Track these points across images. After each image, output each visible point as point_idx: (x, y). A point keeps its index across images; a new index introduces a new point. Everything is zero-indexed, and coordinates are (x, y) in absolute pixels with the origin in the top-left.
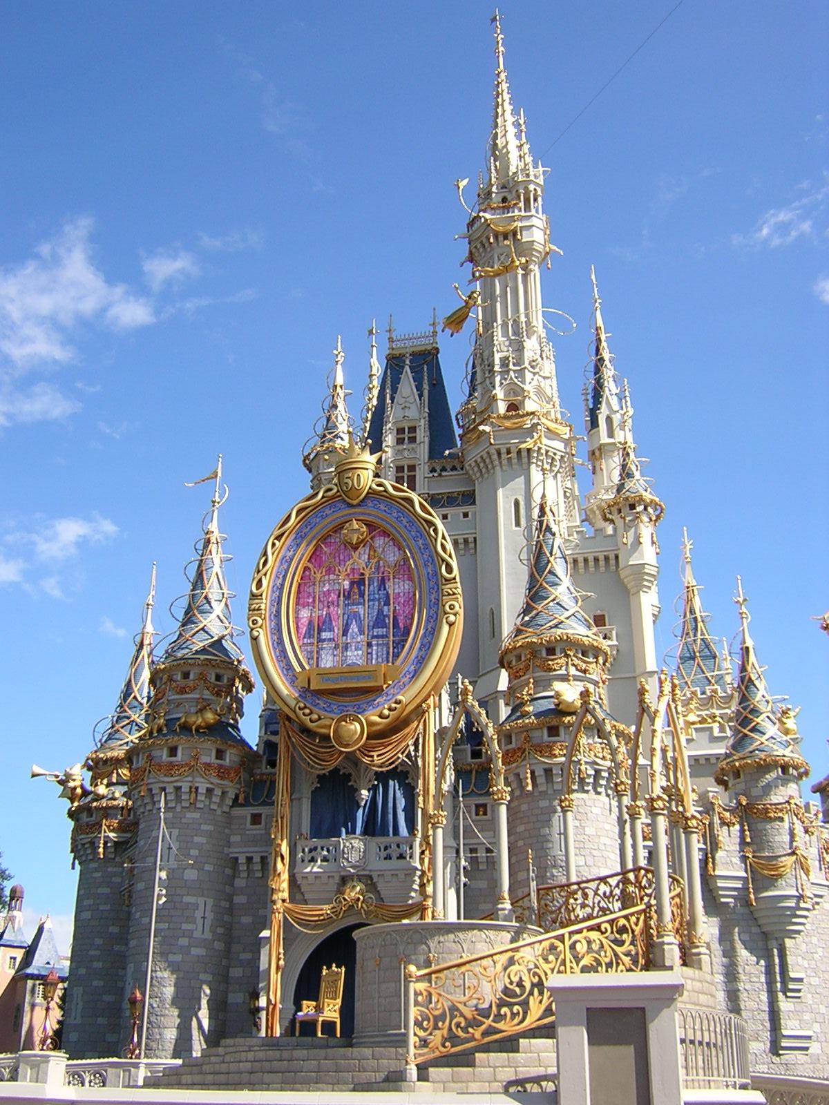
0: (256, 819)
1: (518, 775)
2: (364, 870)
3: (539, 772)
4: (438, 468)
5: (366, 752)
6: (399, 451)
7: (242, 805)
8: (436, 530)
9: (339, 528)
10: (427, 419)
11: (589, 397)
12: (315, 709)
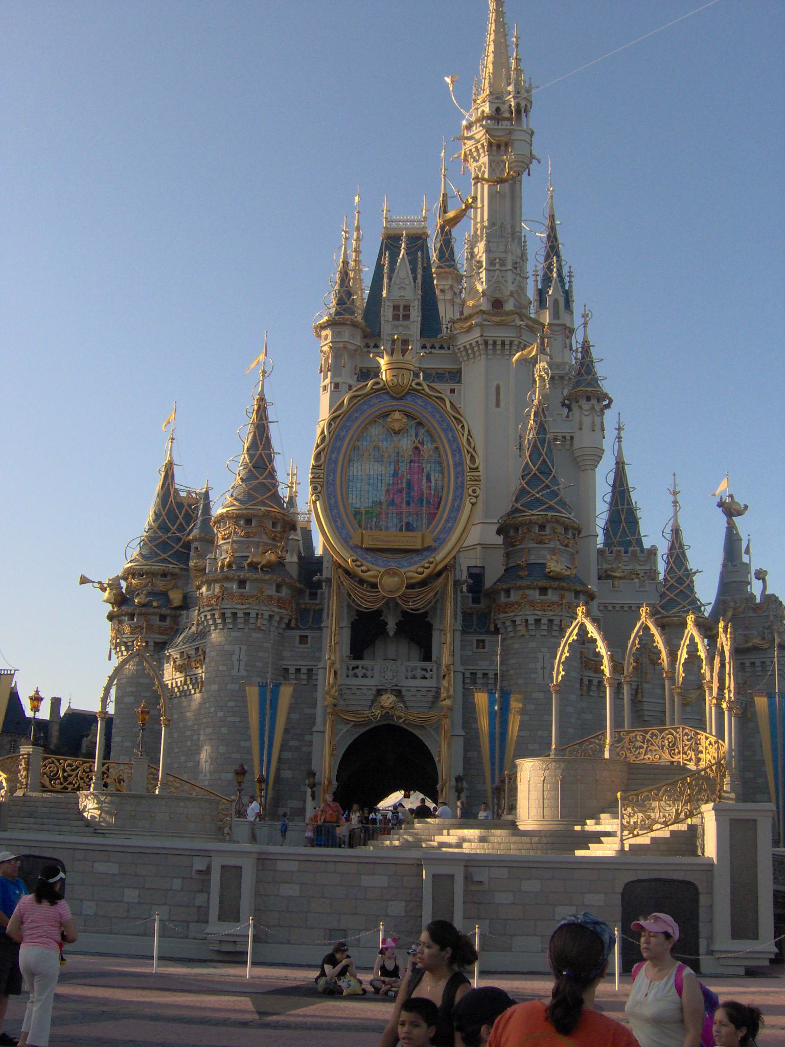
0: (303, 639)
2: (396, 686)
4: (428, 346)
5: (404, 598)
6: (395, 326)
7: (292, 629)
9: (386, 415)
10: (420, 300)
11: (539, 278)
12: (365, 563)
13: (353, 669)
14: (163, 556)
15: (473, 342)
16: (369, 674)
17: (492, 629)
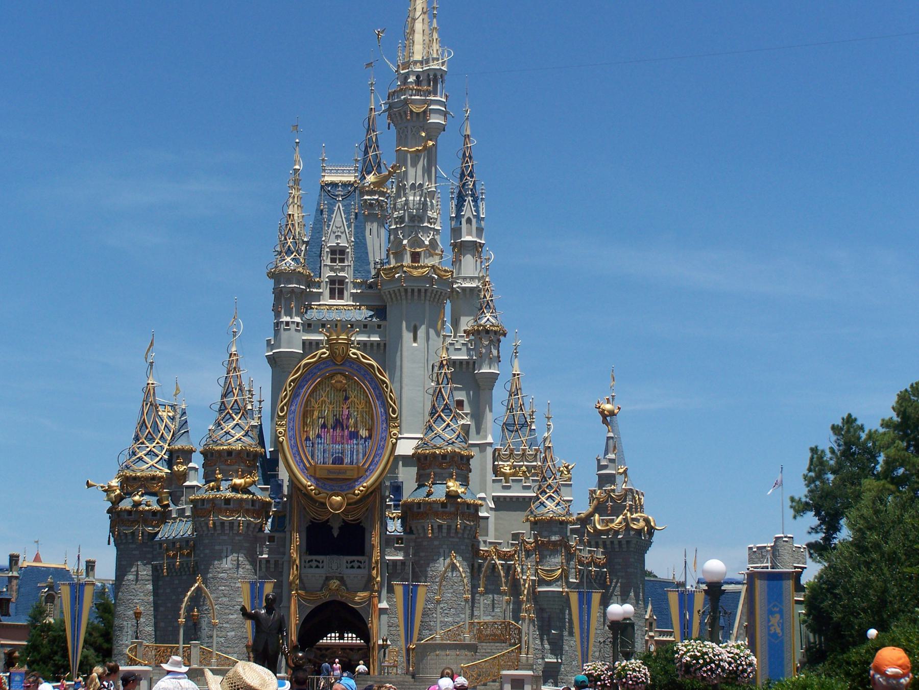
1: (424, 527)
2: (340, 574)
3: (435, 527)
8: (387, 387)
13: (309, 562)
14: (151, 463)
15: (396, 289)
16: (320, 565)
17: (409, 531)
